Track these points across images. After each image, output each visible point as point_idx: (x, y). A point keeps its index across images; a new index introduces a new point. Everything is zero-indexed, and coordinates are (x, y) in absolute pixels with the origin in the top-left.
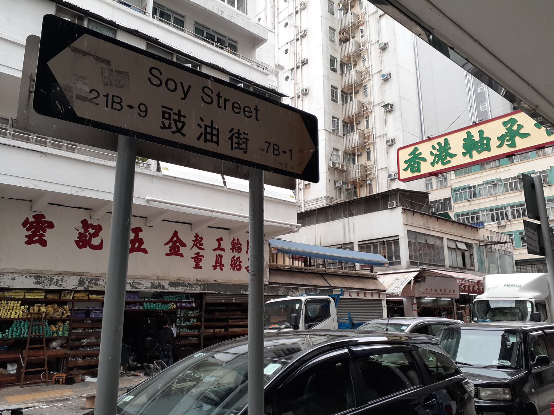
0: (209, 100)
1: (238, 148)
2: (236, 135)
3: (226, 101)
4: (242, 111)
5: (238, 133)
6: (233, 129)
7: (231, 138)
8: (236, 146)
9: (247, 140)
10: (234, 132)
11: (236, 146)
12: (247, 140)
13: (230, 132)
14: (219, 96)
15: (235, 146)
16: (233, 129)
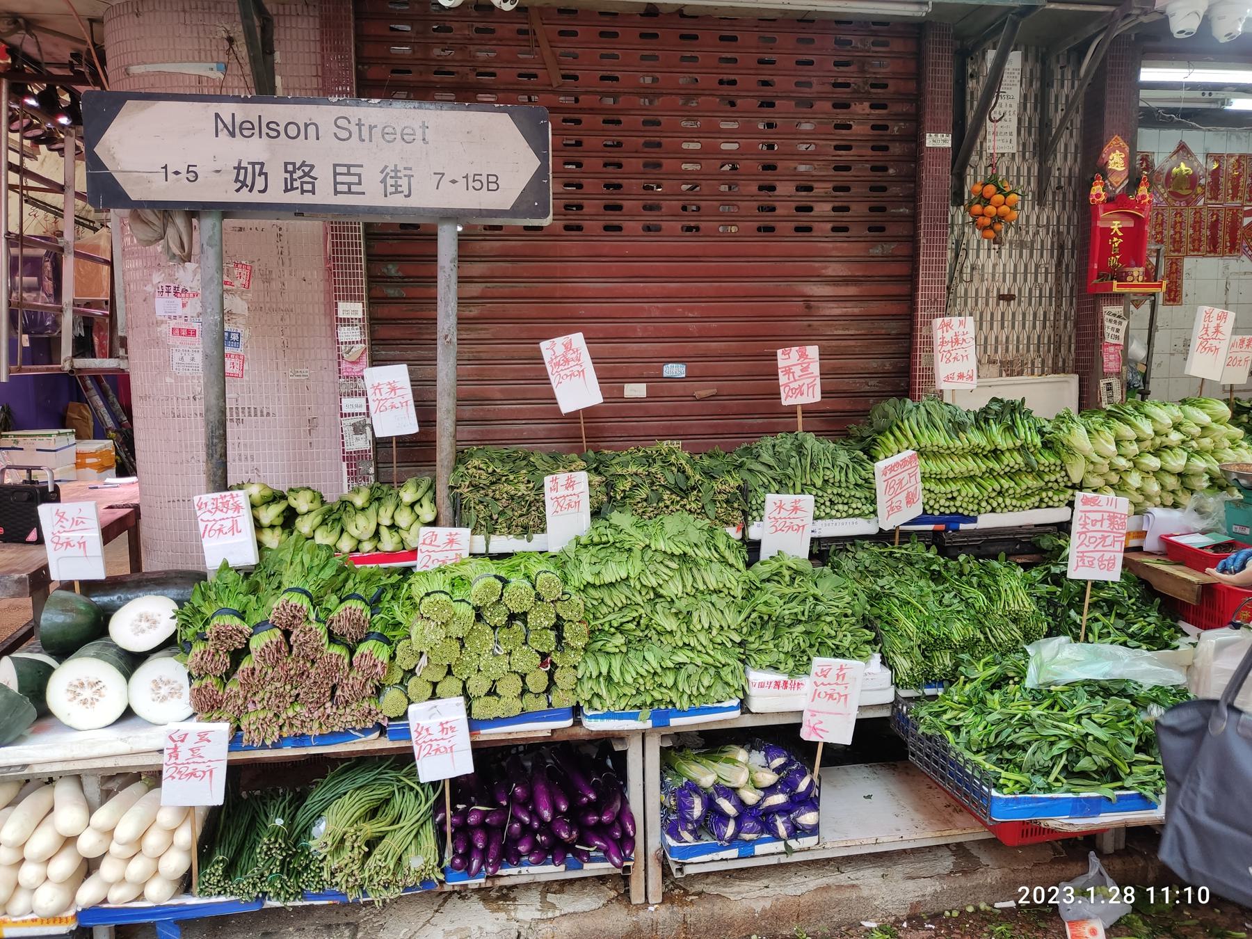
0: (344, 134)
1: (397, 192)
2: (393, 174)
3: (371, 128)
4: (398, 136)
5: (396, 171)
6: (386, 167)
7: (384, 181)
8: (393, 189)
9: (410, 177)
10: (388, 170)
11: (393, 189)
12: (410, 177)
13: (382, 172)
14: (359, 125)
15: (390, 189)
16: (386, 167)
